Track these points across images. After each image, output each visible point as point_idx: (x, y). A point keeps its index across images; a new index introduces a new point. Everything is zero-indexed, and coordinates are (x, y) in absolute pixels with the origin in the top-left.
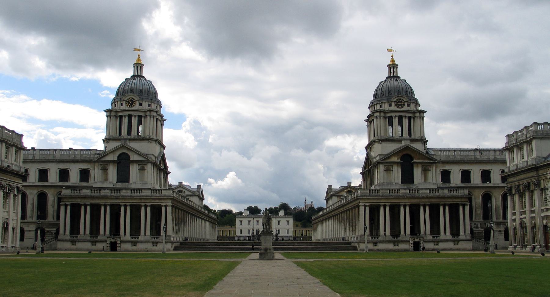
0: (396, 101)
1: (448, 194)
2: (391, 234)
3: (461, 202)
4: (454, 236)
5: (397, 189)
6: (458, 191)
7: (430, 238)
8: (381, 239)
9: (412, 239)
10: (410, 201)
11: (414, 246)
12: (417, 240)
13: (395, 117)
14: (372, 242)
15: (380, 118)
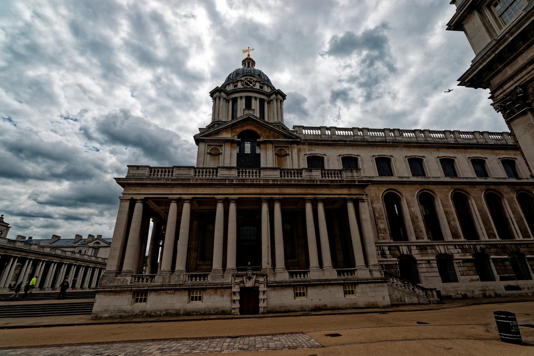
0: (243, 80)
1: (321, 179)
2: (188, 269)
3: (349, 195)
4: (343, 272)
5: (213, 168)
6: (341, 174)
7: (284, 276)
8: (158, 280)
9: (238, 280)
10: (238, 191)
11: (240, 301)
12: (249, 284)
13: (241, 97)
14: (131, 291)
15: (219, 99)
